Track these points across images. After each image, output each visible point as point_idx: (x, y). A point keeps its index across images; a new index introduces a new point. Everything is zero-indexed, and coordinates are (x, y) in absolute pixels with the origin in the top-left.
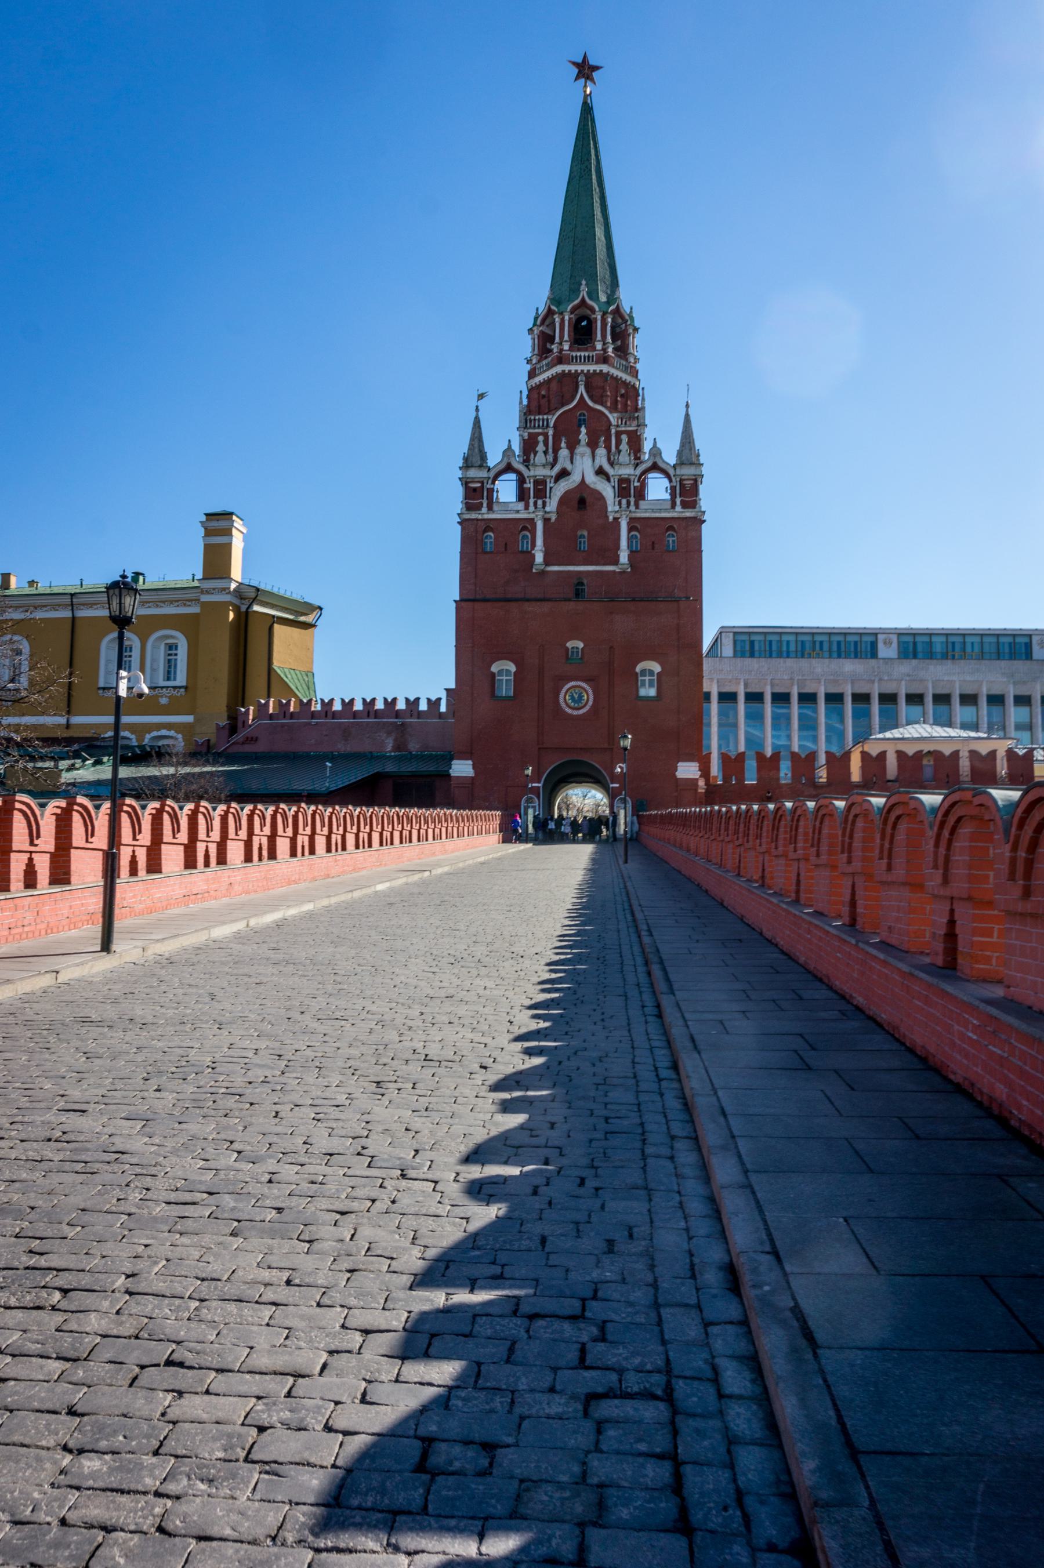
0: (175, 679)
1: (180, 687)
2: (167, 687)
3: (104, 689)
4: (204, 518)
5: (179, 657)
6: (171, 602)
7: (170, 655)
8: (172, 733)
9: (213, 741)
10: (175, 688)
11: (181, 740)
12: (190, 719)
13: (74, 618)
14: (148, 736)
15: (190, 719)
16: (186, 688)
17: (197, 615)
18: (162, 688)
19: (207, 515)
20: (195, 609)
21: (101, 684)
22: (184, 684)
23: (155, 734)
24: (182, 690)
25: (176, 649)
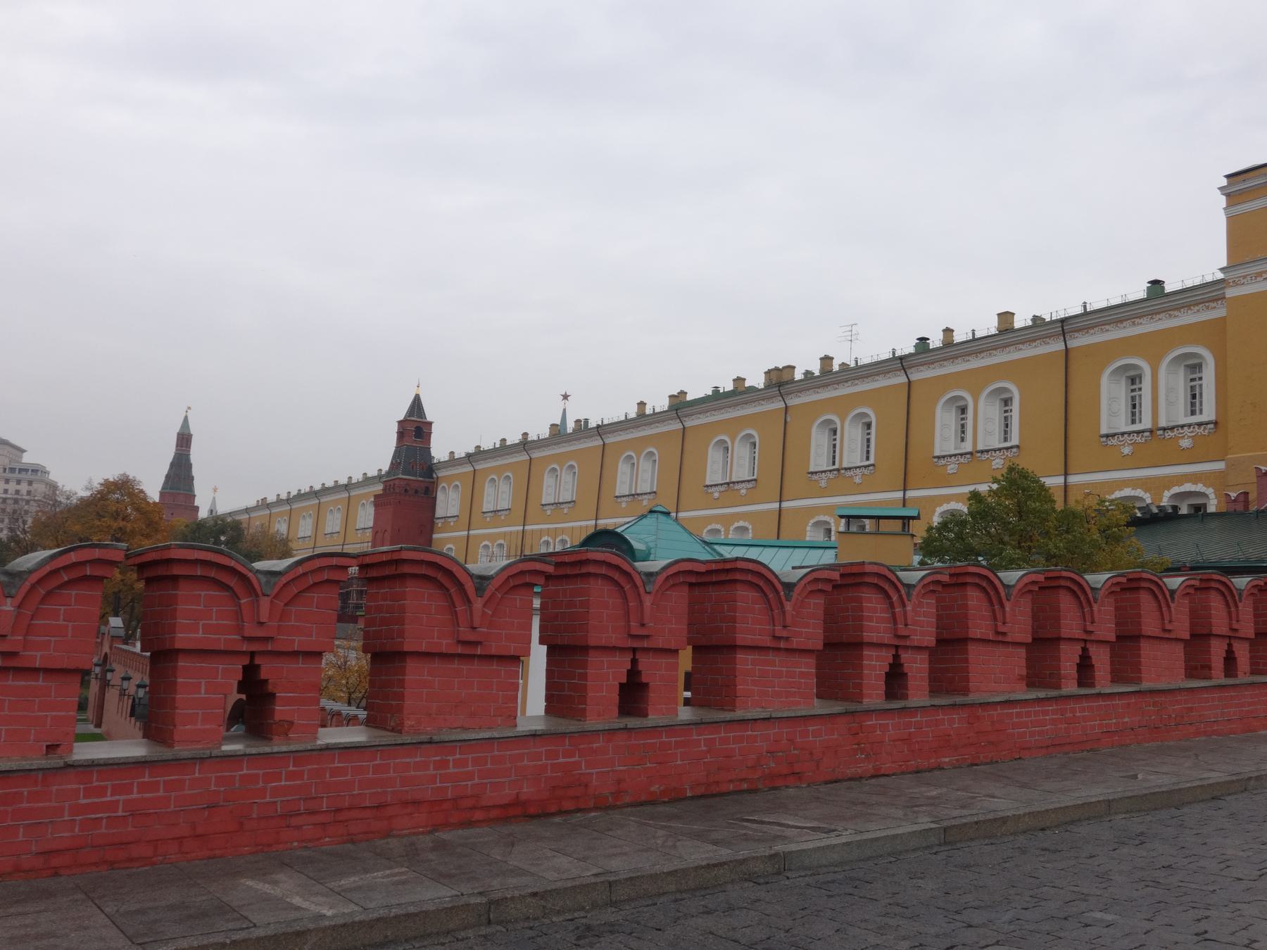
0: (1201, 413)
1: (1207, 423)
2: (1189, 426)
3: (1107, 436)
4: (1224, 182)
5: (1204, 382)
6: (1189, 306)
7: (1192, 380)
8: (1199, 488)
9: (1252, 497)
10: (1200, 424)
11: (1212, 496)
12: (1220, 466)
13: (909, 382)
14: (1167, 494)
15: (1220, 466)
16: (1216, 423)
17: (1223, 320)
18: (1182, 426)
19: (1228, 176)
20: (1219, 312)
21: (1104, 431)
22: (1213, 418)
23: (1176, 490)
24: (1212, 426)
25: (1200, 371)
